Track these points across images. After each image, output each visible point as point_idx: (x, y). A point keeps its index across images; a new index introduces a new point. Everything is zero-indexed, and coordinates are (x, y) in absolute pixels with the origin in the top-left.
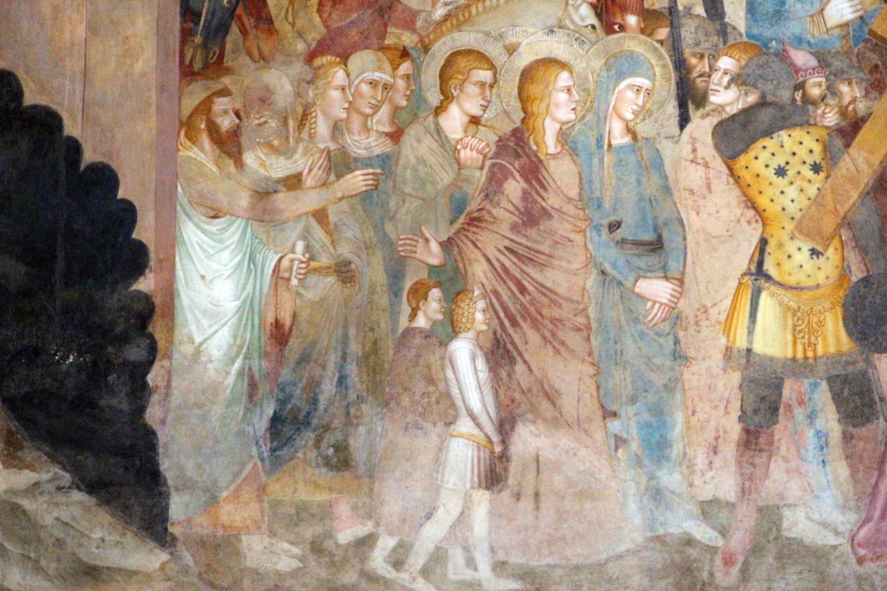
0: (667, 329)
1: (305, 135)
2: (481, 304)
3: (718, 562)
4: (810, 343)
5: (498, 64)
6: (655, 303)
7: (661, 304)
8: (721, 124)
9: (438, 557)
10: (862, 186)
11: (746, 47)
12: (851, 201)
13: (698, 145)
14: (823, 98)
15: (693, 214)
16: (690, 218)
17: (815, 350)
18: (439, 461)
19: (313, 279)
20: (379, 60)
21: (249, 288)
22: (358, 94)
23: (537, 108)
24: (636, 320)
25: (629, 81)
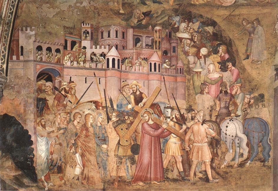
1: (54, 125)
2: (80, 149)
5: (82, 114)
19: (56, 145)
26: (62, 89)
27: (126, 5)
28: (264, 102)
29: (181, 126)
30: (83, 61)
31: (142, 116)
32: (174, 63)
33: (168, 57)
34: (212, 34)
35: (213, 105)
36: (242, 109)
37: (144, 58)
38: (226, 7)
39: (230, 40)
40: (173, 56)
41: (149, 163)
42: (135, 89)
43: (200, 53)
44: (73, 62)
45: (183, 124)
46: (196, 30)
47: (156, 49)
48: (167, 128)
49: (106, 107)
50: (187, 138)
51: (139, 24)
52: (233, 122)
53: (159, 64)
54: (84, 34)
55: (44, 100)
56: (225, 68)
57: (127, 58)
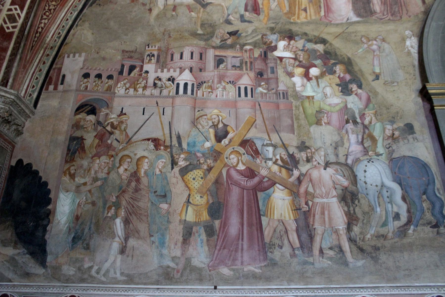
0: (166, 215)
1: (89, 174)
2: (123, 210)
3: (175, 272)
4: (200, 218)
6: (164, 209)
9: (108, 271)
11: (187, 153)
13: (175, 174)
14: (204, 163)
15: (174, 189)
16: (173, 190)
17: (201, 220)
18: (110, 248)
19: (86, 205)
20: (107, 158)
21: (72, 208)
22: (101, 165)
23: (140, 167)
24: (159, 214)
25: (161, 160)
26: (108, 123)
27: (206, 26)
28: (415, 135)
29: (290, 172)
30: (143, 88)
31: (227, 158)
32: (273, 86)
33: (264, 79)
34: (322, 52)
35: (338, 140)
36: (385, 145)
37: (230, 82)
38: (337, 25)
39: (349, 59)
41: (239, 234)
42: (216, 121)
43: (310, 74)
44: (129, 90)
45: (294, 169)
46: (301, 48)
47: (247, 70)
48: (268, 176)
49: (171, 146)
51: (222, 44)
52: (373, 163)
53: (252, 89)
54: (148, 57)
55: (80, 140)
56: (348, 91)
57: (205, 82)
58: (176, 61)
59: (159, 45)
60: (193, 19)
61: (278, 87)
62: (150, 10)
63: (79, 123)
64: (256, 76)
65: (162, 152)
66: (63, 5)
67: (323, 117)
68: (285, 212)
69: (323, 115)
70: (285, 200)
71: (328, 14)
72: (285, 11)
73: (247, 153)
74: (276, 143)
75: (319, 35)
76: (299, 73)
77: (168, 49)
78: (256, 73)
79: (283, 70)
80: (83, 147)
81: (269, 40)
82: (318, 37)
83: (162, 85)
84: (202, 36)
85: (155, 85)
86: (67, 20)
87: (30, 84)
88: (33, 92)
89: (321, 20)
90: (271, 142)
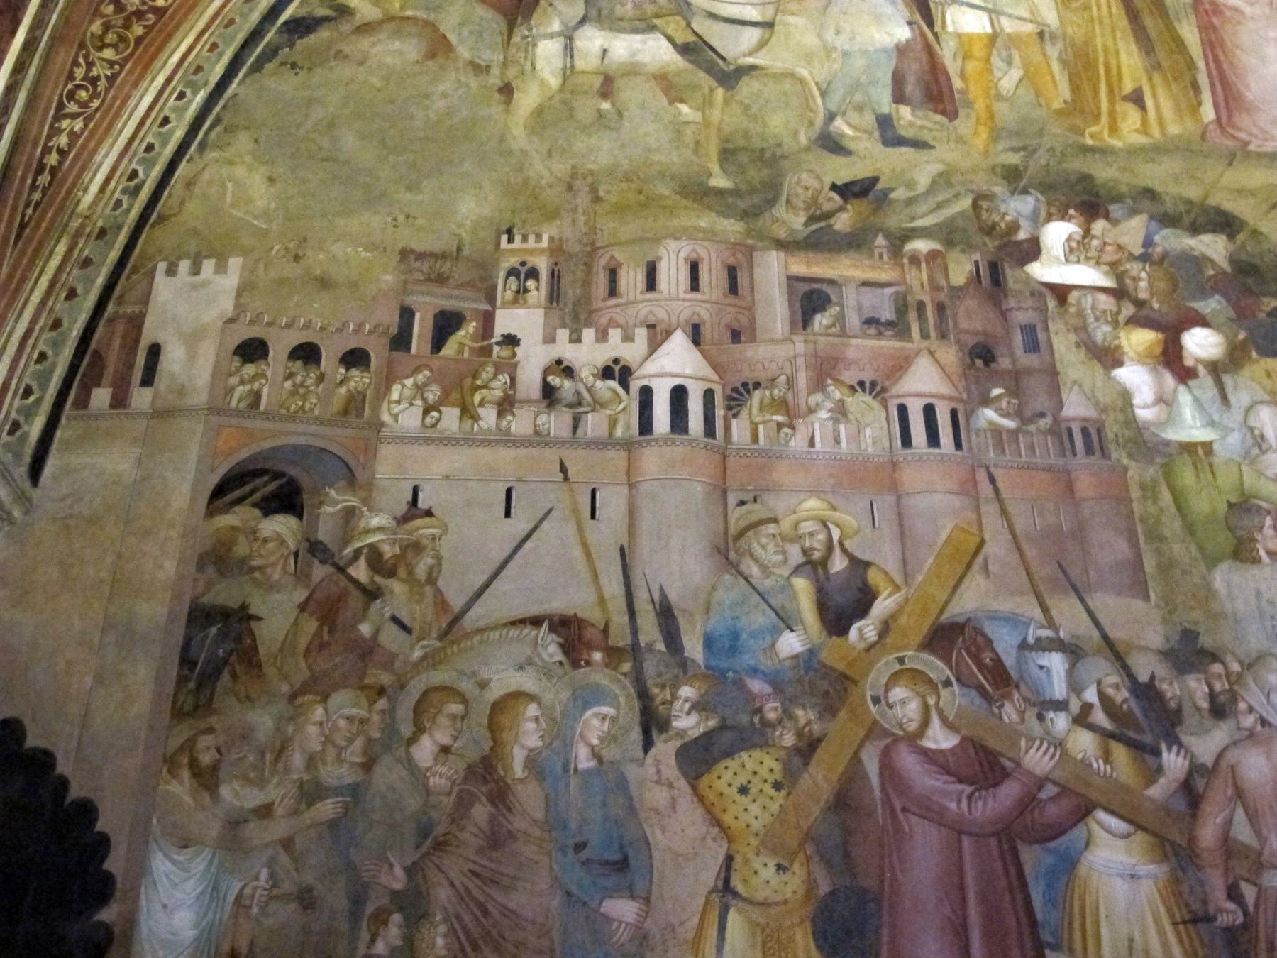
1: (280, 767)
2: (442, 929)
6: (621, 923)
7: (627, 924)
8: (684, 746)
10: (822, 803)
11: (705, 676)
12: (814, 817)
13: (663, 768)
14: (780, 721)
15: (658, 833)
16: (656, 837)
19: (274, 906)
20: (357, 697)
21: (210, 915)
22: (335, 728)
25: (595, 710)
26: (357, 553)
27: (744, 158)
29: (1150, 759)
31: (876, 700)
32: (1041, 402)
34: (1226, 266)
40: (1029, 371)
43: (1185, 354)
44: (440, 412)
45: (1164, 747)
46: (1138, 251)
47: (925, 335)
48: (1057, 775)
49: (635, 651)
50: (1208, 834)
51: (813, 232)
53: (954, 414)
57: (757, 385)
58: (632, 298)
59: (555, 232)
60: (689, 131)
61: (1060, 405)
62: (507, 91)
63: (230, 550)
64: (968, 361)
65: (597, 673)
66: (146, 66)
67: (1261, 529)
68: (1144, 932)
69: (1257, 520)
70: (1139, 877)
71: (1230, 117)
72: (1057, 104)
73: (958, 680)
74: (1078, 638)
75: (1206, 197)
76: (1141, 348)
77: (593, 250)
78: (966, 351)
79: (1073, 338)
80: (250, 658)
81: (1003, 218)
82: (1204, 209)
83: (578, 393)
84: (730, 200)
85: (549, 393)
86: (166, 121)
87: (14, 382)
88: (29, 413)
89: (1203, 136)
90: (1057, 632)
